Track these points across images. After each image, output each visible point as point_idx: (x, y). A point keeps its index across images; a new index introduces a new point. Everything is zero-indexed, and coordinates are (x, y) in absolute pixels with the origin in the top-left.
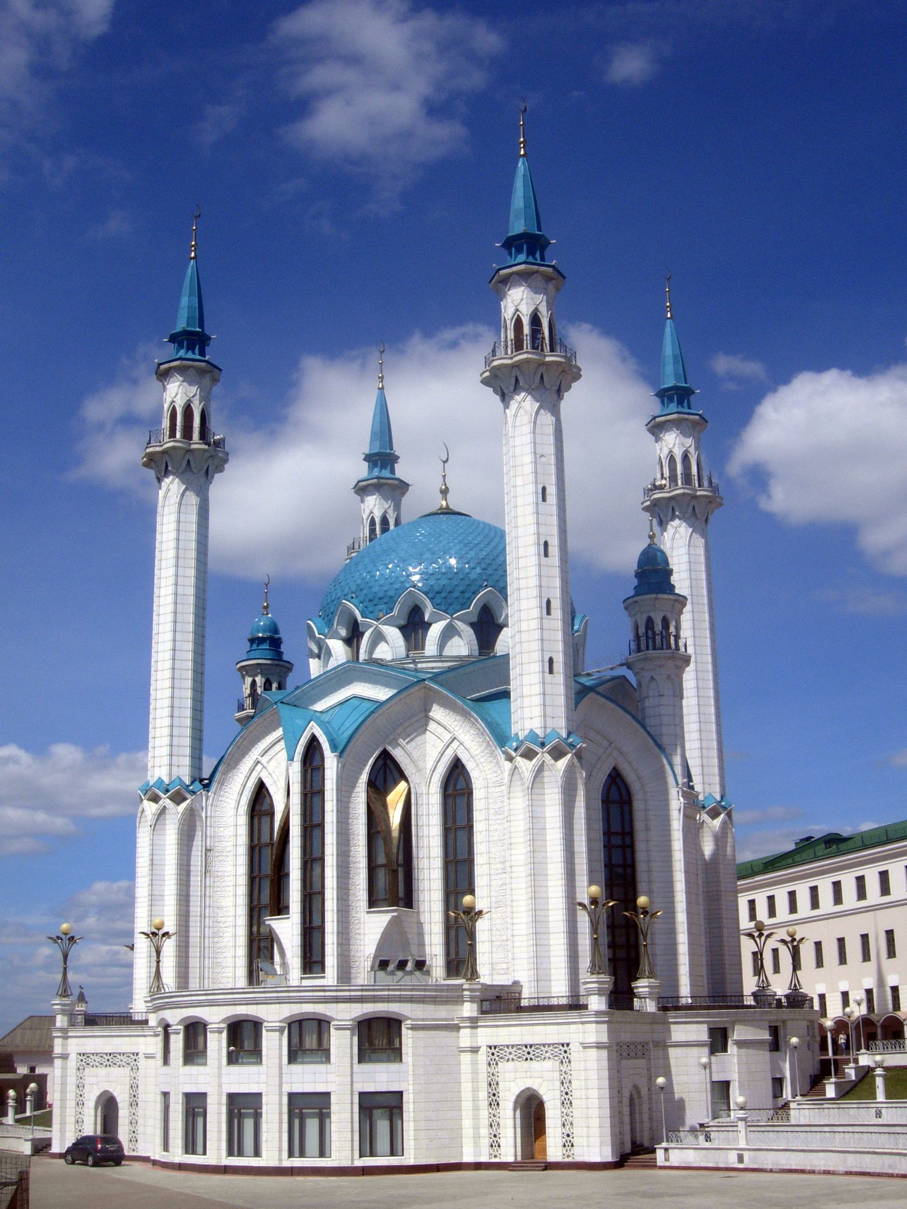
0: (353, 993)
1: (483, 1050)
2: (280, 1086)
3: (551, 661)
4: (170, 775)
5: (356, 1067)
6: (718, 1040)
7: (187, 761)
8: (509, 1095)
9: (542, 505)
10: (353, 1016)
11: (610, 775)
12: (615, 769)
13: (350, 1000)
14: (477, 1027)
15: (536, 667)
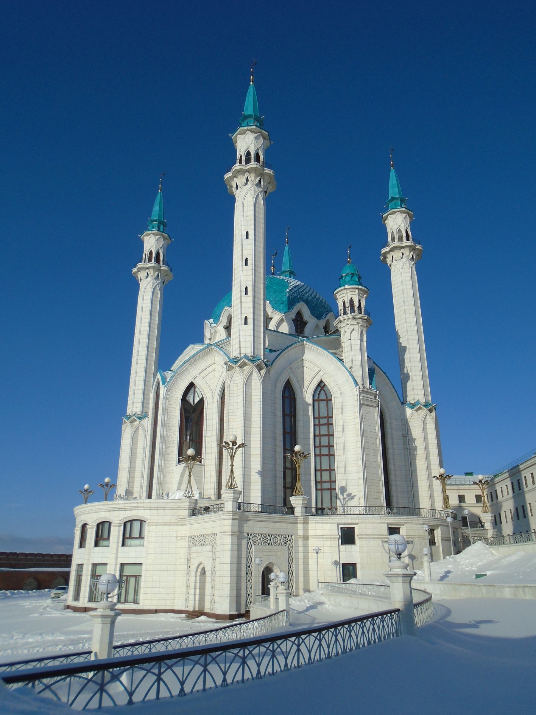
0: (120, 506)
1: (187, 537)
2: (89, 560)
3: (246, 318)
4: (132, 412)
5: (121, 549)
6: (348, 536)
7: (140, 405)
8: (193, 568)
9: (246, 241)
10: (121, 518)
11: (319, 385)
12: (321, 382)
13: (119, 510)
14: (186, 525)
15: (238, 323)
